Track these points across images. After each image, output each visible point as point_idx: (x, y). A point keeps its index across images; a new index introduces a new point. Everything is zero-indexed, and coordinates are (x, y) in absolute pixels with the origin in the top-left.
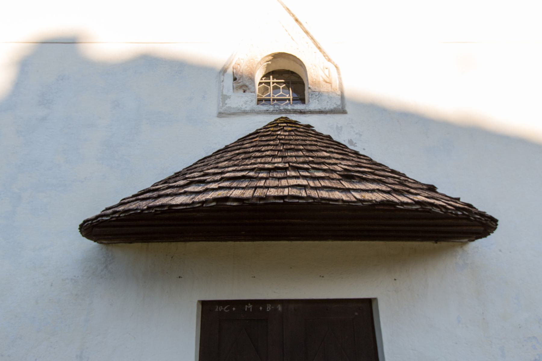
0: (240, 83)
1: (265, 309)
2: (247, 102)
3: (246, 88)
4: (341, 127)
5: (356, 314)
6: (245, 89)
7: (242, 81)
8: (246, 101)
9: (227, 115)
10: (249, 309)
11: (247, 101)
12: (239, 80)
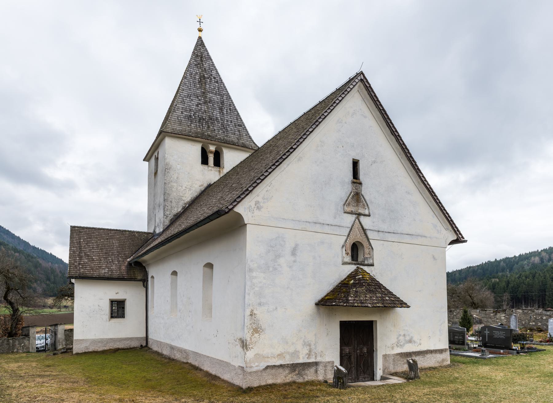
1: (351, 323)
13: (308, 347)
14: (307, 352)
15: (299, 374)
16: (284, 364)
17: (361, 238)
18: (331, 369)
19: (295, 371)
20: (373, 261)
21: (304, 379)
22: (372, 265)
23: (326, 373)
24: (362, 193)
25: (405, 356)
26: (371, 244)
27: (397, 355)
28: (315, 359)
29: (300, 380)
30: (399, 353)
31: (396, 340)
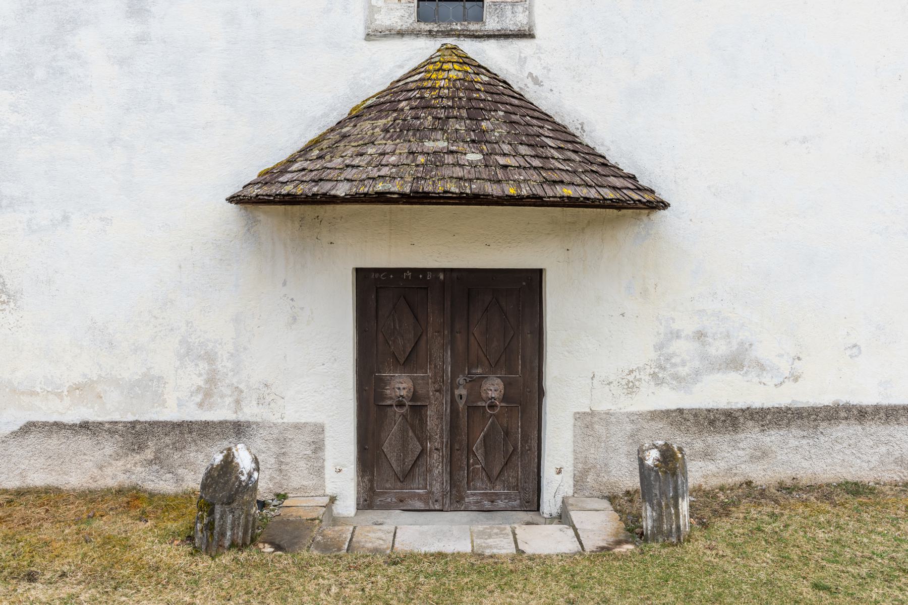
1: (425, 277)
4: (525, 58)
5: (524, 284)
10: (407, 277)
13: (203, 366)
14: (201, 383)
15: (157, 460)
16: (100, 419)
18: (309, 452)
19: (141, 448)
20: (531, 14)
21: (179, 480)
22: (525, 34)
23: (283, 467)
25: (697, 423)
27: (653, 419)
28: (236, 412)
29: (161, 482)
30: (664, 408)
31: (653, 355)
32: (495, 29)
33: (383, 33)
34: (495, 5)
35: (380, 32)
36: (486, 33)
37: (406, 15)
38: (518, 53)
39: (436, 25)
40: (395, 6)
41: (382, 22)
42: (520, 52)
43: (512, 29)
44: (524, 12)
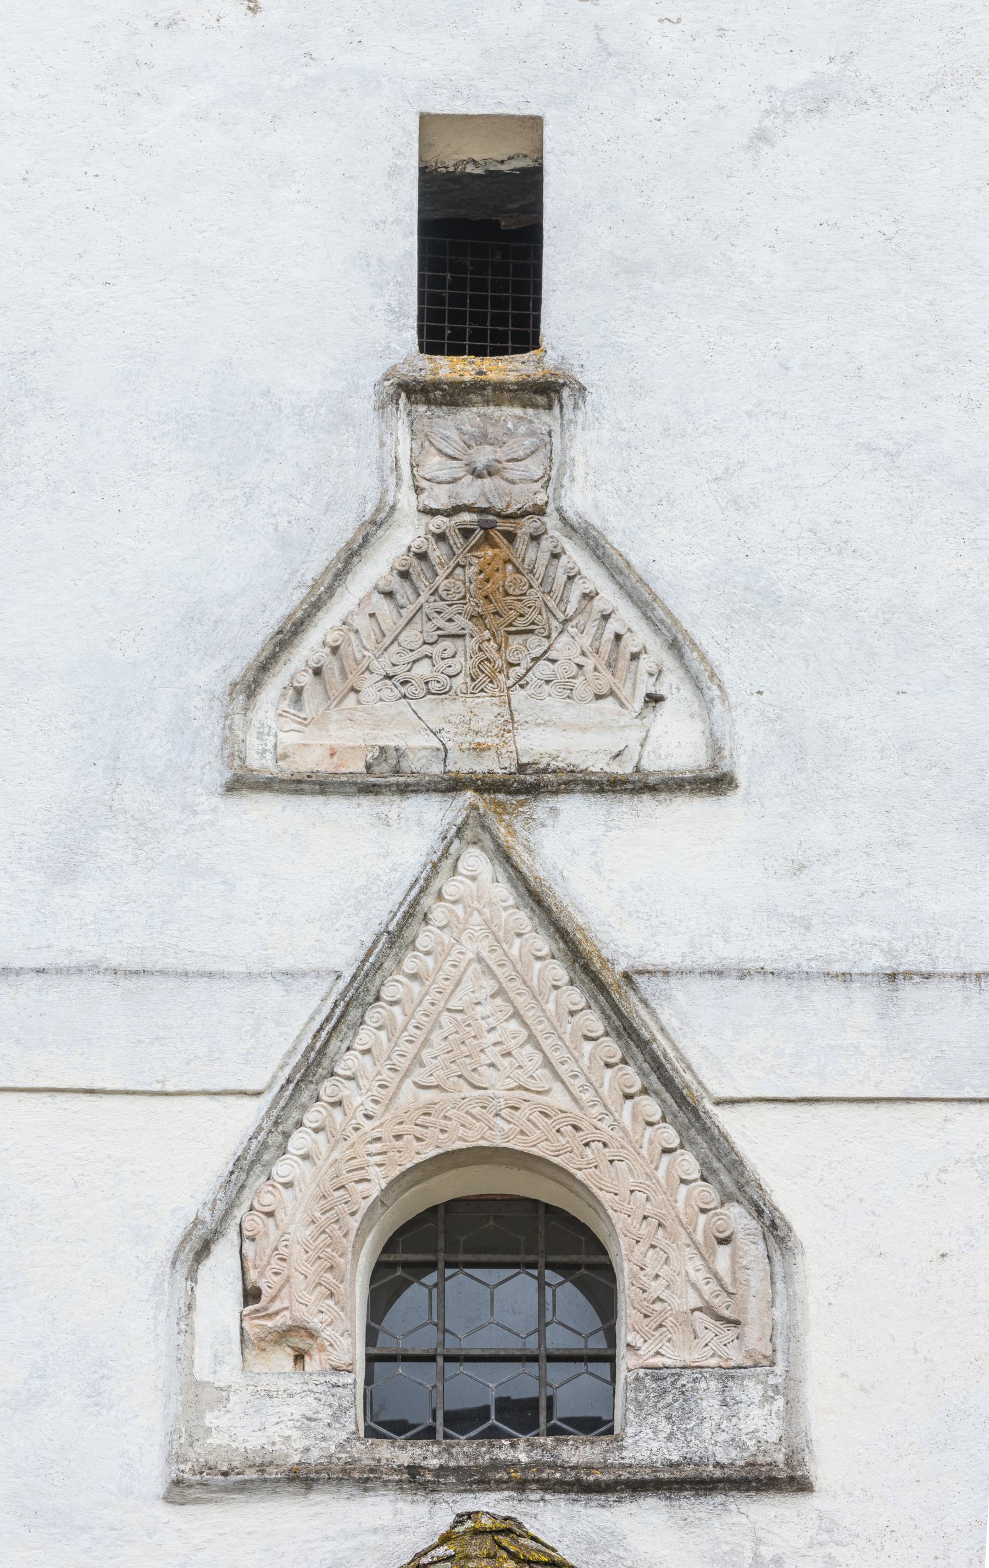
0: (277, 1313)
2: (313, 1424)
3: (310, 1341)
4: (777, 1560)
6: (301, 1345)
7: (286, 1304)
8: (304, 1416)
9: (214, 1492)
11: (310, 1419)
12: (273, 1299)
17: (558, 1098)
24: (565, 504)
26: (736, 1165)
32: (659, 1459)
33: (233, 1478)
34: (657, 1379)
35: (225, 1474)
36: (625, 1475)
37: (325, 1414)
38: (749, 1545)
39: (436, 1449)
40: (282, 1383)
41: (233, 1437)
42: (758, 1541)
43: (724, 1460)
44: (767, 1399)
